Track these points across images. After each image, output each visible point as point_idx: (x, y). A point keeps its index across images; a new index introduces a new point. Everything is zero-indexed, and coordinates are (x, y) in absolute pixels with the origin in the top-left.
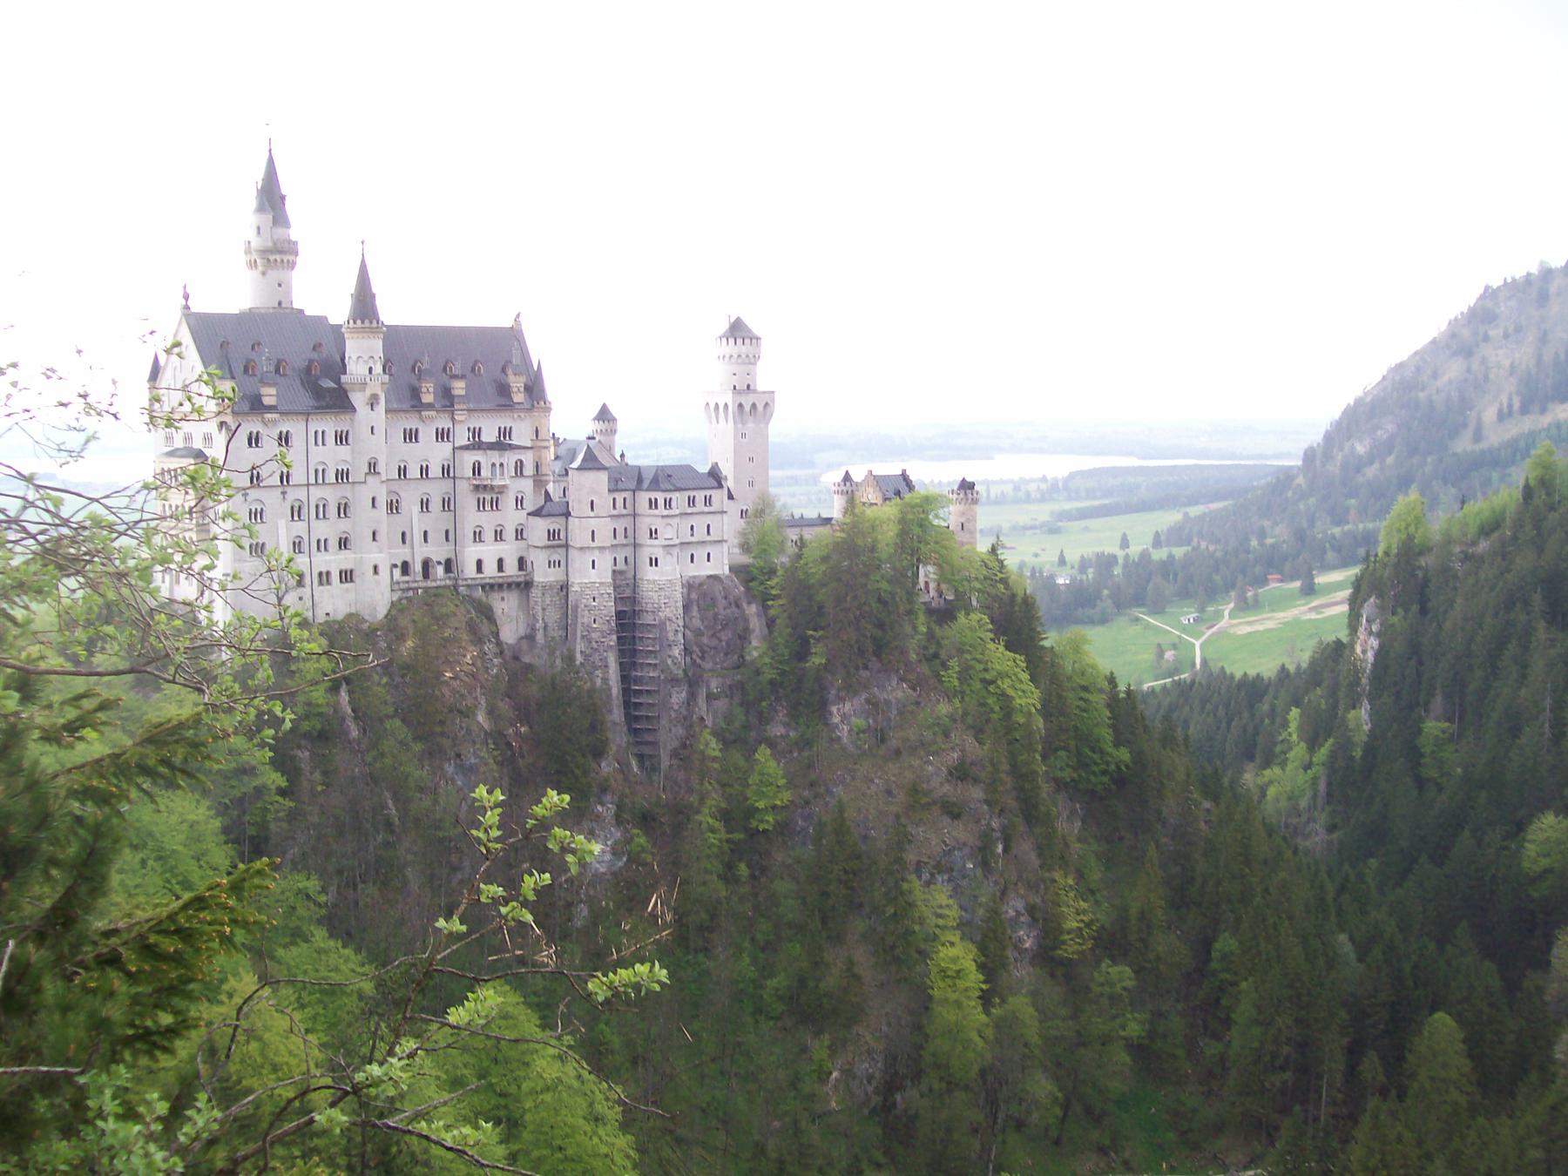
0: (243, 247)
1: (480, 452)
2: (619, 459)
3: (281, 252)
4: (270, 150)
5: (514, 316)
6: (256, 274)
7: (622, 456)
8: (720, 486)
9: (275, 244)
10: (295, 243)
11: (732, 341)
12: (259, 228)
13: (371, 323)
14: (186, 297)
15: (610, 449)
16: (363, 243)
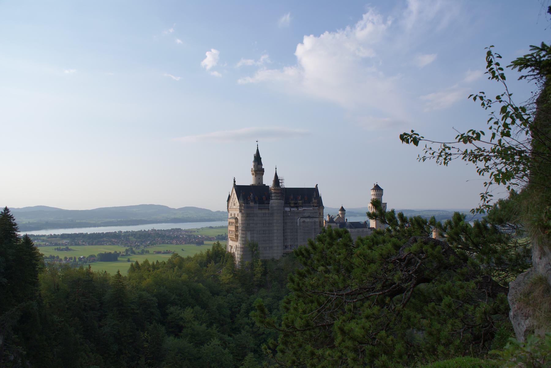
0: (251, 170)
1: (305, 218)
2: (345, 221)
3: (260, 171)
4: (258, 148)
5: (315, 185)
6: (254, 176)
7: (347, 220)
8: (367, 228)
9: (258, 169)
10: (264, 169)
11: (375, 190)
12: (254, 166)
13: (277, 187)
14: (235, 182)
15: (343, 217)
16: (276, 168)
